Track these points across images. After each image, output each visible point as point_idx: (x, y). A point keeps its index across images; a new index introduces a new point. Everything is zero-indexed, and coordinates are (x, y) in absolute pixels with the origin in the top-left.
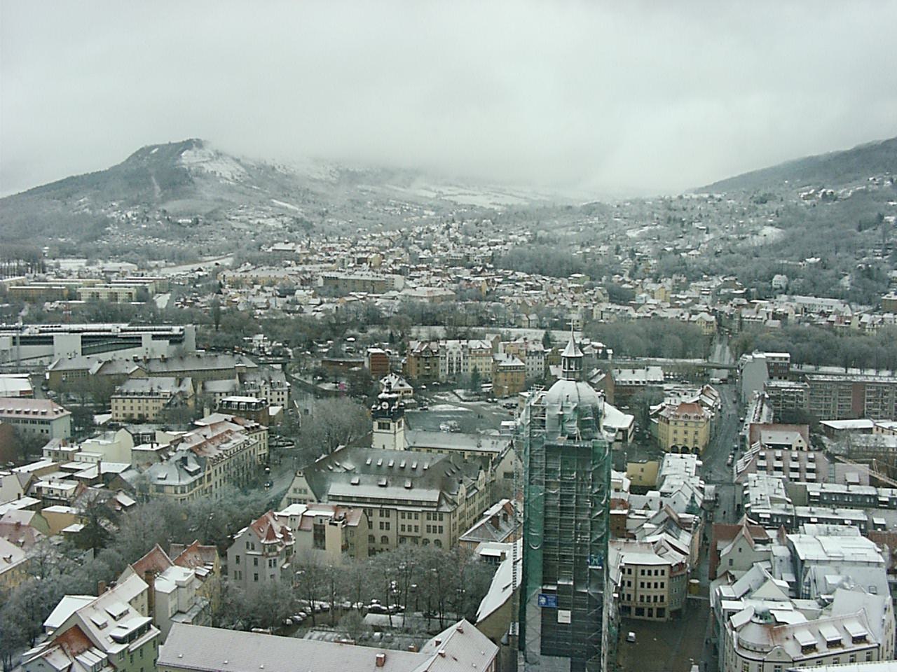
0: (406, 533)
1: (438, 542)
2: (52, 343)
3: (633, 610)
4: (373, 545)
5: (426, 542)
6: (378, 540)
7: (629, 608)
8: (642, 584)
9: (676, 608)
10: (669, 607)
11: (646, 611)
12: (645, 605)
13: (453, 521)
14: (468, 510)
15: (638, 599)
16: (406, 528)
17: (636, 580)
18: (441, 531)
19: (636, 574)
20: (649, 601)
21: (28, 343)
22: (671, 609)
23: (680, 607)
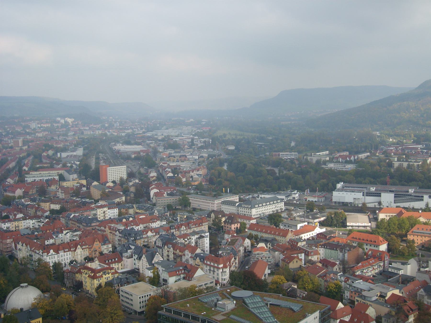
2: (380, 196)
21: (370, 196)
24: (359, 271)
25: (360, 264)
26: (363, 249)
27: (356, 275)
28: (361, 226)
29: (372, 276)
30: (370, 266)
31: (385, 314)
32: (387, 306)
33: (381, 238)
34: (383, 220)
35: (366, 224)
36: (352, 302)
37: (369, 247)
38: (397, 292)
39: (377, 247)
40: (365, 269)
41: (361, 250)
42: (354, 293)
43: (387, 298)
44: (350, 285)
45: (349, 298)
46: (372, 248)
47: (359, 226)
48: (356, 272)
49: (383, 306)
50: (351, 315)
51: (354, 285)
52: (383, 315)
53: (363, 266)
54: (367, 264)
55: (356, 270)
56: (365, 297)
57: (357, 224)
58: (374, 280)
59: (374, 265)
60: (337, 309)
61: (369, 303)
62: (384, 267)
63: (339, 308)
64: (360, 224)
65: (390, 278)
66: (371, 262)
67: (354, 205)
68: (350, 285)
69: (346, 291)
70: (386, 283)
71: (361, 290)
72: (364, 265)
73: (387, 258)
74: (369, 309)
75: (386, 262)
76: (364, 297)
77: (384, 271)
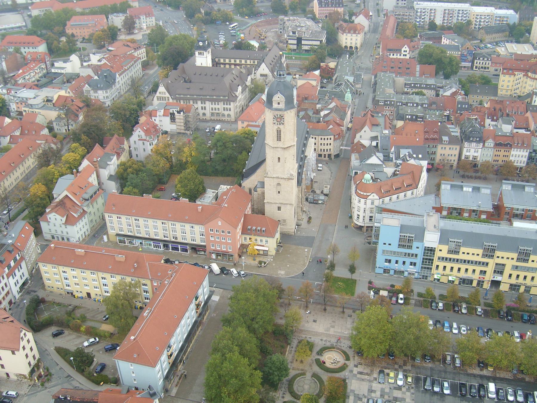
0: (214, 111)
1: (229, 115)
5: (223, 115)
6: (201, 115)
9: (337, 153)
10: (333, 153)
11: (323, 156)
13: (235, 105)
15: (319, 150)
16: (214, 109)
18: (230, 110)
20: (324, 151)
22: (335, 154)
23: (338, 153)
24: (22, 79)
25: (21, 71)
26: (21, 53)
27: (19, 84)
28: (15, 28)
29: (36, 82)
30: (32, 71)
31: (56, 118)
32: (55, 110)
33: (39, 39)
34: (36, 17)
35: (20, 25)
36: (20, 113)
37: (27, 50)
38: (63, 93)
39: (35, 48)
40: (27, 75)
41: (18, 55)
42: (20, 103)
43: (54, 102)
44: (13, 96)
45: (16, 110)
46: (31, 50)
47: (12, 28)
48: (18, 81)
49: (51, 110)
50: (20, 128)
51: (18, 95)
52: (53, 119)
53: (24, 73)
54: (28, 69)
55: (17, 78)
56: (31, 105)
57: (11, 26)
58: (38, 86)
59: (36, 68)
60: (5, 125)
61: (37, 111)
62: (47, 69)
63: (7, 124)
64: (14, 26)
65: (55, 79)
66: (32, 66)
67: (3, 4)
68: (14, 97)
69: (11, 104)
70: (51, 85)
71: (27, 99)
72: (25, 71)
73: (47, 58)
74: (38, 117)
75: (48, 63)
76: (31, 106)
77: (48, 73)
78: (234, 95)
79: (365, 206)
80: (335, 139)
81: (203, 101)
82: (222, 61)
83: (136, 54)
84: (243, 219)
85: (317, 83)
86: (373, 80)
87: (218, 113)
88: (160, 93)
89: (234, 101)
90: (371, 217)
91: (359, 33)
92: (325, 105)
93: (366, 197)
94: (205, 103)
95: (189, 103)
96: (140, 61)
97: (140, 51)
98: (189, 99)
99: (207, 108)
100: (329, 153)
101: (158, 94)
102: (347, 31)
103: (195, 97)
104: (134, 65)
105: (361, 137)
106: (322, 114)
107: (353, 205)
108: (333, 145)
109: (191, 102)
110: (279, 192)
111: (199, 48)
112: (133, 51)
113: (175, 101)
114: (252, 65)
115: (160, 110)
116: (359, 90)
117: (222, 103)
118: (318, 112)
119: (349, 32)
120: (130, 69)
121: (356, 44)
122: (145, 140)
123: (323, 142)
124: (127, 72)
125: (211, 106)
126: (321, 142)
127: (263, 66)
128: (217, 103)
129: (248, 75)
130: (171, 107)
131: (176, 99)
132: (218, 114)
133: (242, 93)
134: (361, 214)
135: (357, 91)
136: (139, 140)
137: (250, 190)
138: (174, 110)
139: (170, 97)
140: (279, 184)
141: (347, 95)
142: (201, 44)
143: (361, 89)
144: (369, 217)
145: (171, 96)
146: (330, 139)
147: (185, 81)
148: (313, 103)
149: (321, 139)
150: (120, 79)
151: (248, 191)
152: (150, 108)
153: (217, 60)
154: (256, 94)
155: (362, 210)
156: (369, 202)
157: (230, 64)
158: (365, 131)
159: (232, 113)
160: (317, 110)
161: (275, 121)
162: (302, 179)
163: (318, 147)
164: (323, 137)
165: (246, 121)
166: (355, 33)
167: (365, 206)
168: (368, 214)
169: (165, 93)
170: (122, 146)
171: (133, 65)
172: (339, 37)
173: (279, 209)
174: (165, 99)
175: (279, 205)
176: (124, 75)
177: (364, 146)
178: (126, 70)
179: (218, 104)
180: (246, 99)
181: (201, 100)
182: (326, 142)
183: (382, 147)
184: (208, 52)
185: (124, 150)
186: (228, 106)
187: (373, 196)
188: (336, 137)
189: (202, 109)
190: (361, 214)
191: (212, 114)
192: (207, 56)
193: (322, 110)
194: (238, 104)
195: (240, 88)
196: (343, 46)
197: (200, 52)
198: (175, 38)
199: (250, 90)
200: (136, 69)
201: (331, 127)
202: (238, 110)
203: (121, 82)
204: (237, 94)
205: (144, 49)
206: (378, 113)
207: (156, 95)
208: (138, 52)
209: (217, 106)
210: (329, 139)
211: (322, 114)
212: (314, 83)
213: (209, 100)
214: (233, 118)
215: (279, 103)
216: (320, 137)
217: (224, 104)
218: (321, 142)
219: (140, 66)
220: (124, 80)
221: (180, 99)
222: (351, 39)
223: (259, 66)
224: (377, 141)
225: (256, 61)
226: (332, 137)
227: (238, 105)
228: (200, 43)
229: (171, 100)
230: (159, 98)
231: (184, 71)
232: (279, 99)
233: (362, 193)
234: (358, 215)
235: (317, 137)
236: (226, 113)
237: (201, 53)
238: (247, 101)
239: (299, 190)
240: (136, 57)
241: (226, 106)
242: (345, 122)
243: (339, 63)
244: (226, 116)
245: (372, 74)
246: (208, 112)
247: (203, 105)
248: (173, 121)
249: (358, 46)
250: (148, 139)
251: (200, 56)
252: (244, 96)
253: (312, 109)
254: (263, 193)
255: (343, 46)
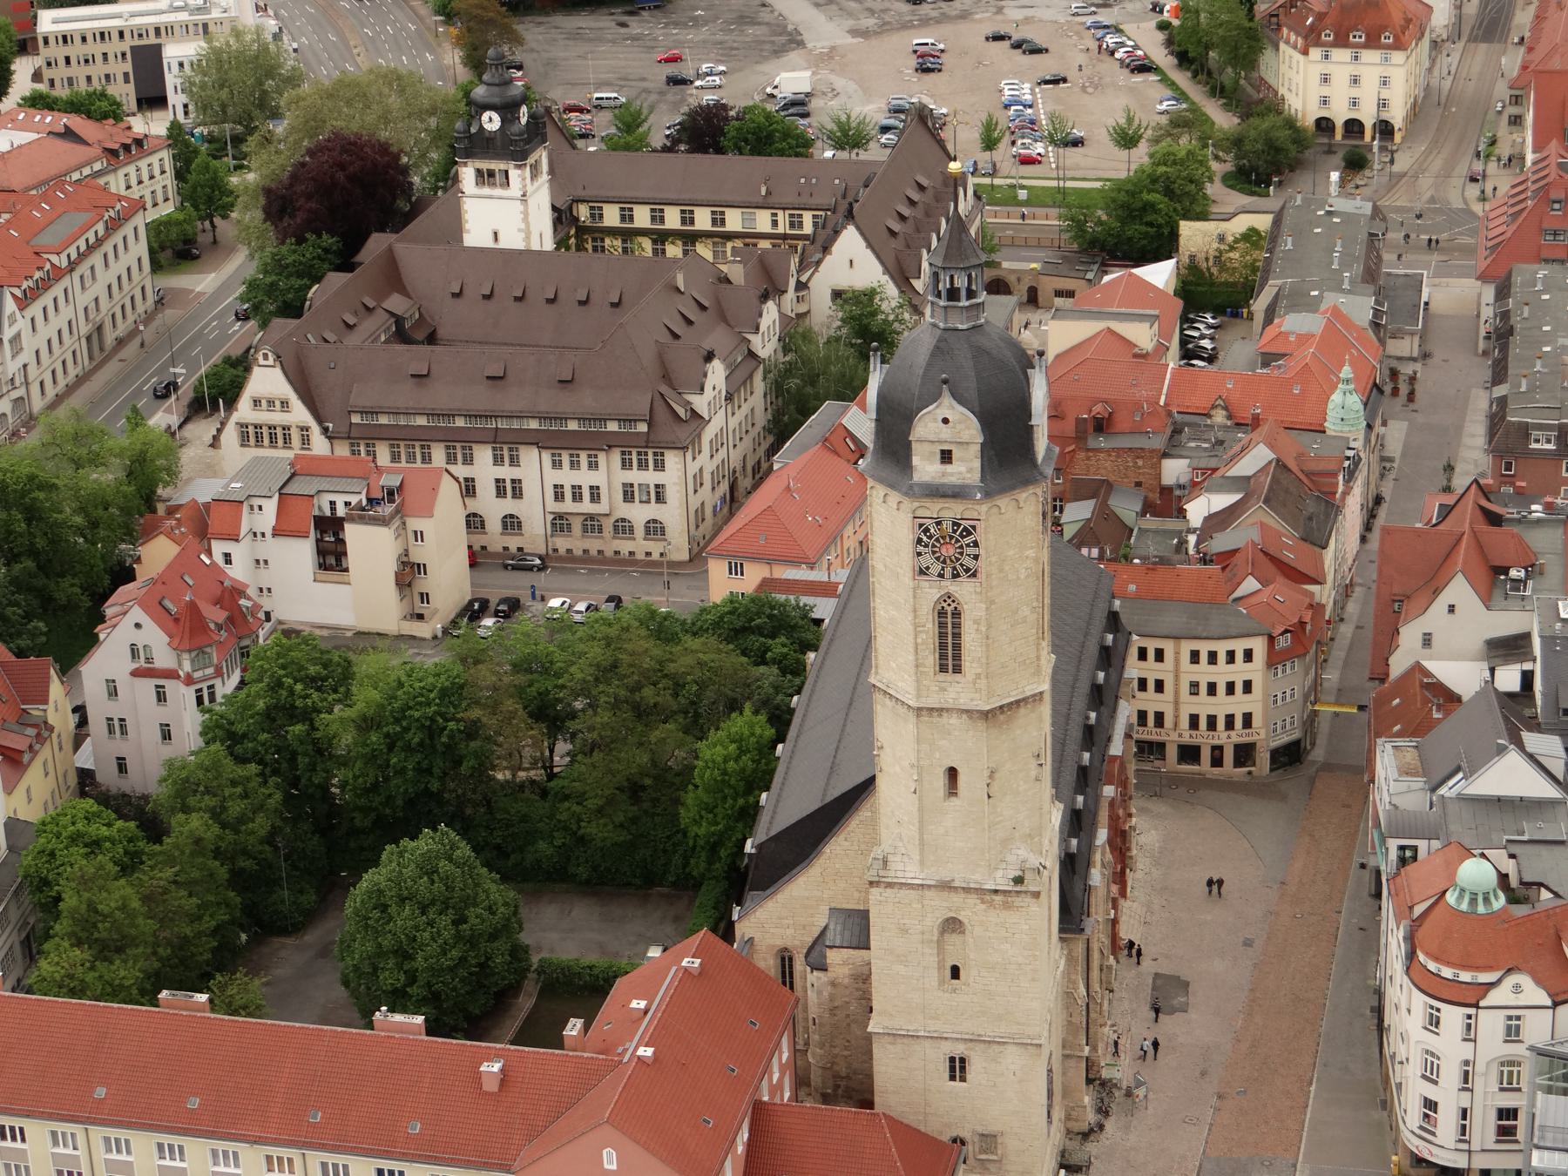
0: (568, 506)
1: (655, 529)
3: (1172, 753)
4: (479, 541)
5: (623, 528)
6: (494, 525)
7: (1161, 746)
8: (1195, 686)
12: (1204, 739)
13: (693, 468)
14: (733, 422)
15: (1185, 722)
17: (1177, 677)
18: (660, 498)
19: (1177, 661)
78: (681, 412)
79: (1467, 1051)
80: (1275, 659)
81: (507, 445)
82: (612, 216)
83: (115, 183)
84: (744, 1135)
85: (1164, 334)
86: (1487, 312)
87: (592, 517)
88: (256, 402)
89: (684, 449)
90: (1507, 1114)
91: (1398, 45)
92: (1213, 463)
93: (1471, 998)
94: (514, 461)
95: (427, 458)
96: (140, 221)
97: (143, 164)
98: (421, 440)
99: (531, 488)
100: (1238, 735)
101: (244, 411)
102: (1328, 36)
103: (460, 422)
104: (108, 247)
105: (1427, 640)
106: (1198, 510)
107: (1393, 1044)
108: (1266, 694)
109: (438, 454)
110: (955, 972)
111: (479, 145)
112: (97, 166)
113: (343, 450)
114: (785, 237)
115: (256, 502)
116: (1407, 369)
117: (616, 457)
118: (1167, 503)
119: (1341, 42)
120: (83, 268)
121: (1383, 104)
122: (171, 674)
123: (1204, 673)
124: (66, 282)
125: (553, 477)
126: (1190, 672)
127: (850, 241)
128: (583, 458)
129: (765, 297)
130: (324, 484)
131: (351, 436)
132: (592, 524)
133: (729, 398)
134: (1449, 1097)
135: (1394, 374)
136: (136, 673)
137: (786, 961)
138: (340, 500)
139: (315, 430)
140: (952, 925)
141: (1336, 397)
142: (491, 122)
143: (1418, 366)
144: (1493, 1115)
145: (319, 419)
146: (1248, 655)
147: (402, 335)
148: (1137, 452)
149: (1195, 657)
150: (22, 324)
151: (767, 963)
152: (202, 491)
153: (583, 212)
154: (805, 411)
155: (1450, 1075)
156: (1491, 1024)
157: (661, 238)
158: (1452, 609)
159: (673, 515)
160: (1166, 491)
161: (927, 560)
162: (1087, 889)
163: (1177, 703)
164: (1204, 648)
165: (756, 558)
166: (1372, 42)
167: (1467, 1051)
168: (1488, 1099)
169: (285, 404)
170: (35, 711)
171: (100, 242)
172: (1283, 68)
173: (957, 1068)
174: (287, 440)
175: (959, 1050)
176: (47, 299)
177: (1449, 698)
178: (57, 274)
179: (593, 466)
180: (754, 432)
181: (496, 439)
182: (1222, 673)
183: (1552, 695)
184: (535, 169)
185: (43, 730)
186: (650, 477)
187: (1517, 989)
188: (1283, 642)
189: (500, 491)
190: (1449, 1097)
191: (560, 523)
192: (530, 189)
193: (1194, 487)
194: (705, 462)
195: (717, 373)
196: (1309, 121)
197: (485, 165)
198: (348, 91)
199: (777, 388)
200: (118, 268)
201: (1250, 585)
202: (709, 497)
203: (30, 343)
204: (700, 403)
205: (166, 155)
206: (1524, 498)
207: (236, 417)
208: (131, 169)
209: (585, 478)
210: (1239, 656)
211: (1198, 510)
212: (1142, 335)
213: (538, 441)
214: (679, 549)
215: (946, 457)
216: (1187, 647)
217: (626, 465)
218: (1190, 672)
219: (141, 249)
220: (47, 331)
221: (371, 436)
222: (1355, 81)
223: (824, 242)
224: (1527, 666)
225: (807, 218)
226: (1259, 646)
227: (710, 467)
228: (486, 116)
229: (320, 445)
230: (252, 435)
231: (393, 278)
232: (946, 433)
233: (1447, 972)
234: (1431, 1105)
235: (1168, 647)
236: (639, 514)
237: (491, 174)
238: (757, 443)
239: (1070, 959)
240: (120, 198)
241: (635, 476)
242: (1329, 556)
243: (1287, 220)
244: (640, 531)
245: (1483, 277)
246: (534, 511)
247: (507, 472)
248: (331, 560)
249: (1397, 115)
250: (187, 666)
251: (486, 191)
252: (741, 414)
253: (1138, 484)
254: (863, 979)
255: (1309, 121)
